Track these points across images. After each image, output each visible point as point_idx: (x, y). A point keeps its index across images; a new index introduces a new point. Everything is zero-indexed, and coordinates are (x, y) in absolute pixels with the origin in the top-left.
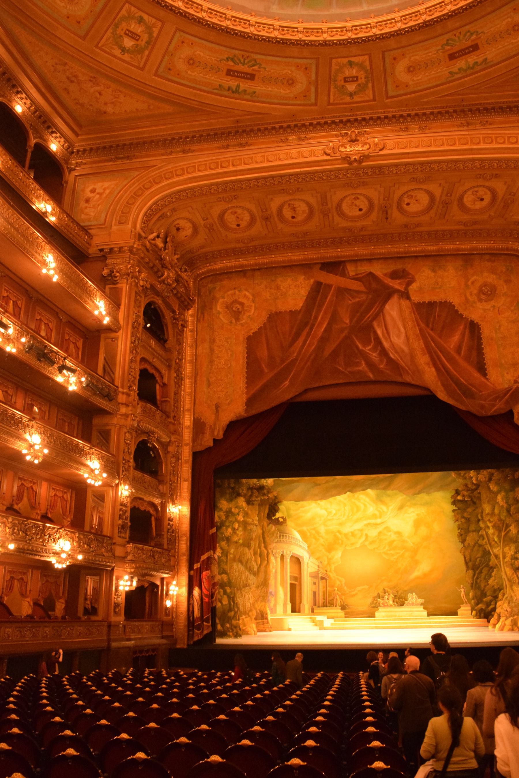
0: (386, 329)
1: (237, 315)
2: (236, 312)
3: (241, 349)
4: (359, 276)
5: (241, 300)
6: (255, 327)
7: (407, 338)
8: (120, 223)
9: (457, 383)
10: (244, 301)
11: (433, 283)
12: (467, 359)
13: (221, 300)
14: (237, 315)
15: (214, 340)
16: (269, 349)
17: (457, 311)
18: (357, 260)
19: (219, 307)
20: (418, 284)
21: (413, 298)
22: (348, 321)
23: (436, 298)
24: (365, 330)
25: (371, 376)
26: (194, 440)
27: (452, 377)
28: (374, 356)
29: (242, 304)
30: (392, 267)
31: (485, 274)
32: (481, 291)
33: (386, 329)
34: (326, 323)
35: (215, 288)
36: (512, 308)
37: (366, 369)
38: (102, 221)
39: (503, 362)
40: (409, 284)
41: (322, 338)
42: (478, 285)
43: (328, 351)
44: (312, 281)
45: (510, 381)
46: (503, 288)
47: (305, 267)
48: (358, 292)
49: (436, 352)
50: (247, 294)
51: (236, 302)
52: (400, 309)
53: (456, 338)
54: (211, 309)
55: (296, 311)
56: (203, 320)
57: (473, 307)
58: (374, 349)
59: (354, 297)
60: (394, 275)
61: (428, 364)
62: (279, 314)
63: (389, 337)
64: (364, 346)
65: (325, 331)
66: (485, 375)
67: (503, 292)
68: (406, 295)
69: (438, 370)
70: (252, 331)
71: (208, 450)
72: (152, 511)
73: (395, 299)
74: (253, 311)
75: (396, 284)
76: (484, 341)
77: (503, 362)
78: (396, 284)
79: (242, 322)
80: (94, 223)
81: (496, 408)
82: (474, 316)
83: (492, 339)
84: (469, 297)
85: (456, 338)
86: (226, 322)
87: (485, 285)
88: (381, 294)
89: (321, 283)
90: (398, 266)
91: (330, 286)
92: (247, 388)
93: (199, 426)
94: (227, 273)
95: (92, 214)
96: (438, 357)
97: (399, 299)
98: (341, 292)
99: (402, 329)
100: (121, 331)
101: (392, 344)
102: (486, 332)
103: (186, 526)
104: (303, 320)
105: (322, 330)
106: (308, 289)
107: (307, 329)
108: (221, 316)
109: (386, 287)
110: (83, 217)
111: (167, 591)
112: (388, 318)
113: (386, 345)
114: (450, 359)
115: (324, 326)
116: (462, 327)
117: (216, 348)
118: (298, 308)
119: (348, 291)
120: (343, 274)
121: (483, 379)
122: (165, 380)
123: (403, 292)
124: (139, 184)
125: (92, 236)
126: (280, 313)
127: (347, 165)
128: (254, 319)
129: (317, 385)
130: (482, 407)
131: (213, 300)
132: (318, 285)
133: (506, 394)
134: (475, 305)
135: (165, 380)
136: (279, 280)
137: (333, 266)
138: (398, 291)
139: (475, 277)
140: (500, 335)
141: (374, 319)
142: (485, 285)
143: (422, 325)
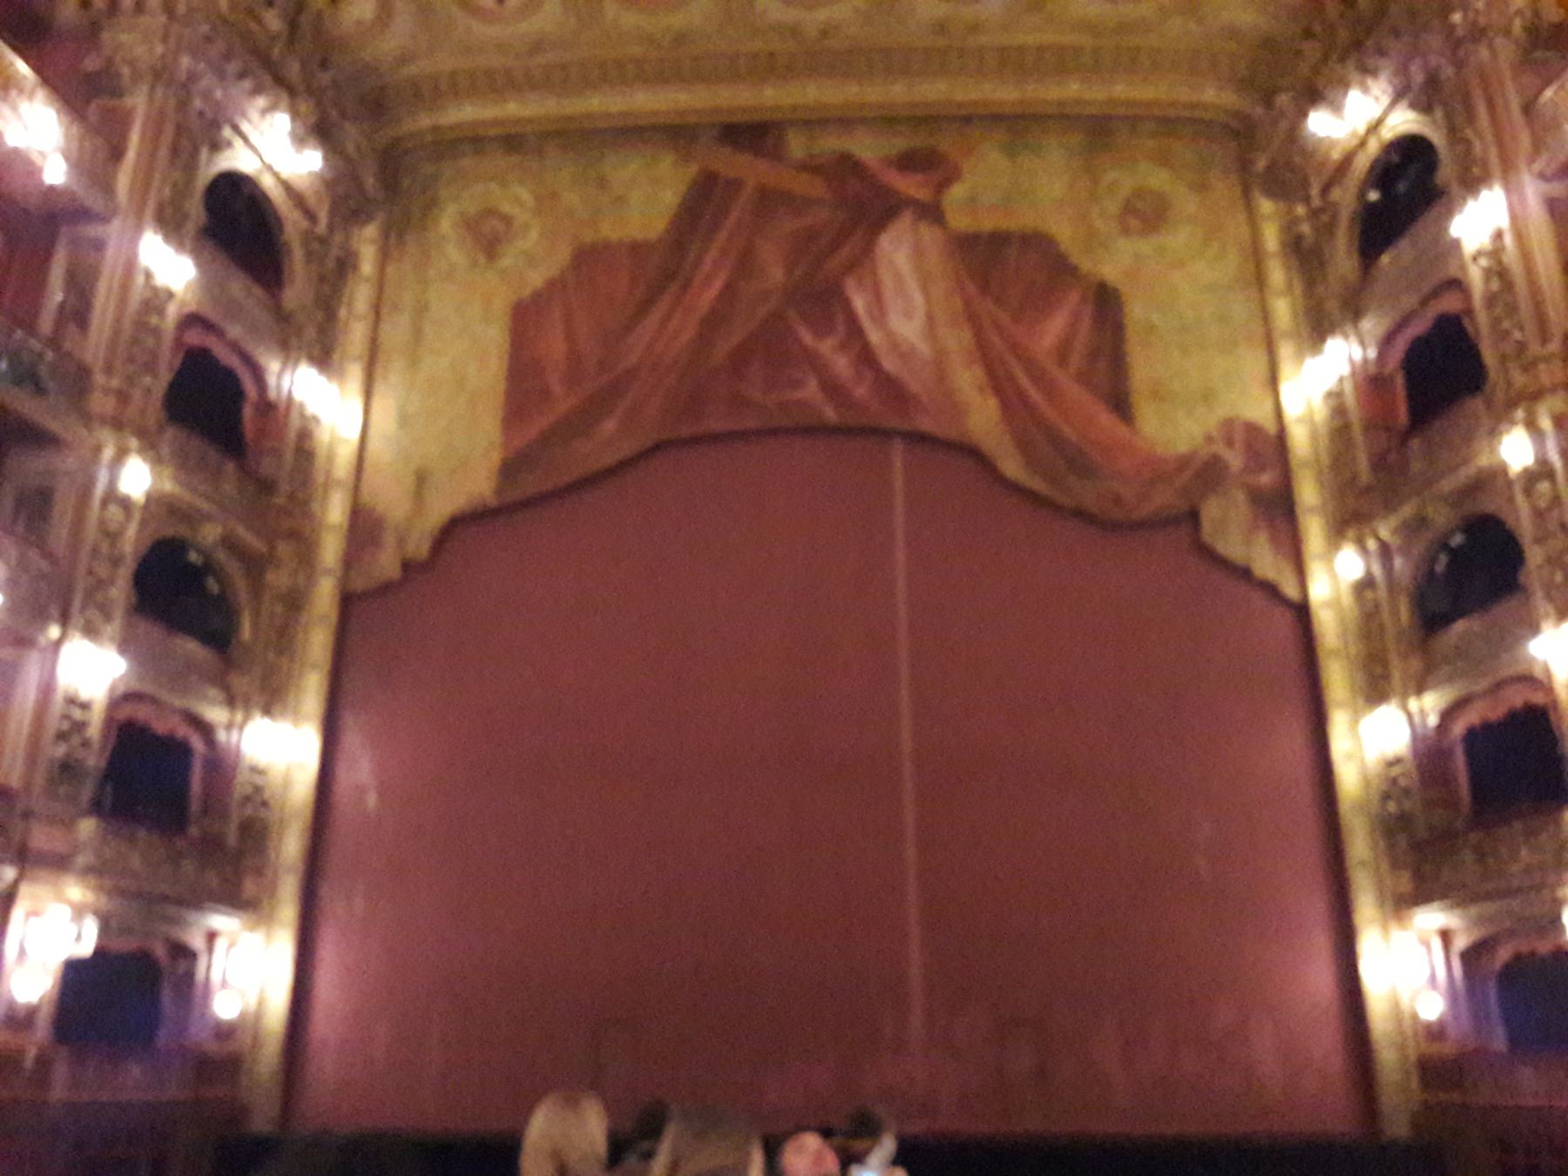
2: (488, 237)
3: (495, 336)
6: (536, 279)
7: (930, 319)
9: (1056, 440)
12: (1084, 378)
16: (570, 337)
18: (815, 121)
19: (446, 222)
24: (822, 300)
26: (350, 560)
28: (842, 365)
29: (507, 220)
30: (899, 144)
32: (1129, 209)
43: (722, 349)
44: (693, 169)
46: (1186, 202)
51: (491, 212)
58: (843, 347)
60: (908, 162)
68: (932, 213)
69: (1006, 406)
75: (911, 186)
85: (1055, 326)
87: (1139, 193)
90: (919, 141)
98: (769, 200)
101: (890, 334)
102: (1136, 312)
104: (663, 266)
107: (674, 288)
113: (874, 336)
114: (1040, 378)
130: (1118, 500)
143: (971, 288)
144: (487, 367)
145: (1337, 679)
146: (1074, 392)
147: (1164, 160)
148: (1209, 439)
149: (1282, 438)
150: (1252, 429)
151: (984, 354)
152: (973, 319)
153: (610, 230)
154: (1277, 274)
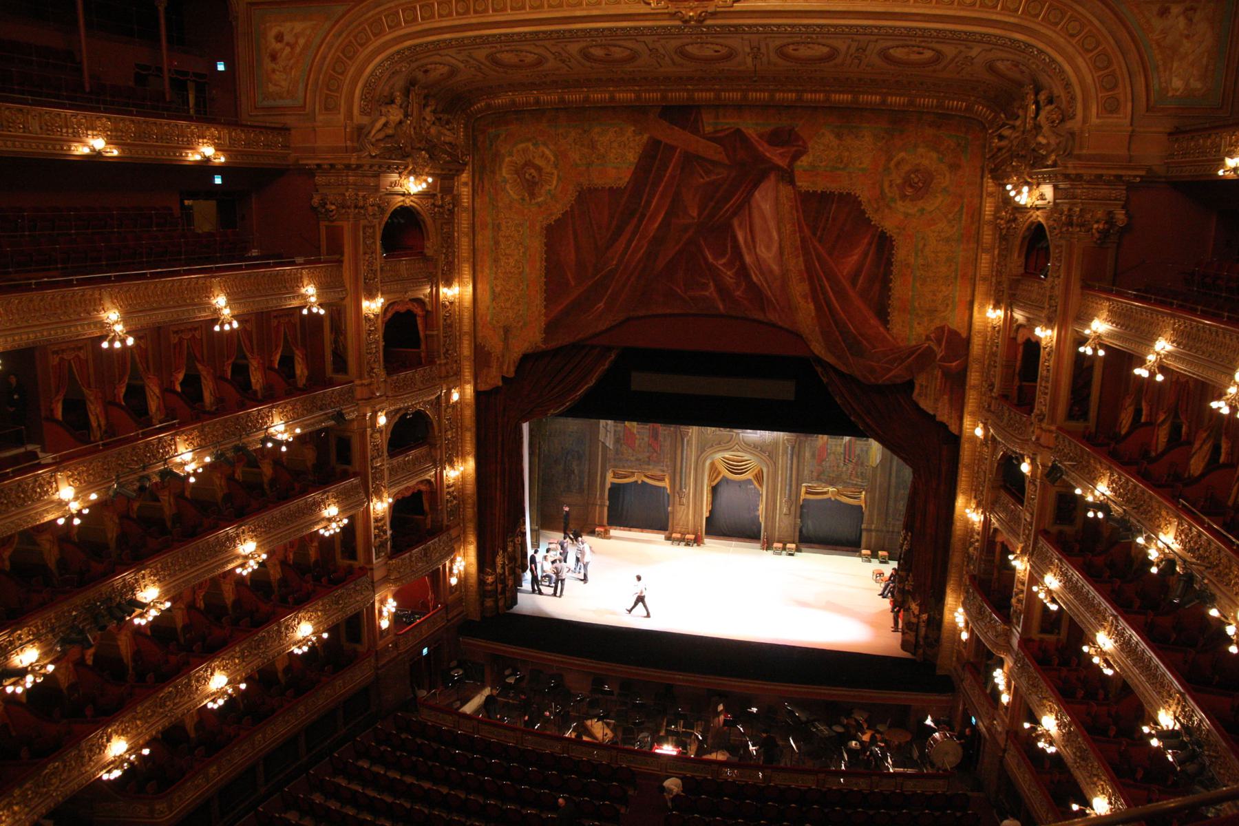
0: (751, 231)
1: (531, 187)
3: (537, 245)
5: (538, 162)
6: (558, 210)
13: (507, 159)
14: (531, 187)
15: (499, 226)
17: (863, 212)
18: (719, 107)
19: (505, 173)
20: (811, 159)
21: (799, 184)
22: (694, 213)
23: (833, 187)
25: (721, 307)
28: (729, 275)
29: (539, 169)
32: (907, 182)
33: (751, 231)
37: (715, 295)
38: (301, 102)
40: (796, 157)
42: (906, 168)
44: (646, 137)
47: (636, 112)
50: (547, 152)
52: (777, 198)
53: (854, 258)
54: (493, 172)
57: (890, 208)
60: (777, 138)
63: (755, 247)
65: (658, 229)
66: (885, 322)
68: (788, 176)
69: (818, 308)
71: (496, 391)
72: (423, 488)
75: (775, 156)
76: (895, 269)
78: (775, 156)
79: (540, 200)
80: (288, 102)
81: (893, 373)
85: (854, 258)
86: (516, 197)
88: (751, 171)
89: (659, 142)
92: (546, 307)
93: (481, 358)
94: (514, 114)
95: (283, 83)
99: (775, 235)
102: (901, 253)
103: (471, 488)
105: (656, 225)
108: (508, 186)
110: (271, 88)
111: (451, 569)
112: (756, 214)
113: (748, 259)
115: (660, 219)
116: (866, 241)
118: (623, 183)
120: (695, 131)
121: (881, 329)
124: (348, 35)
125: (289, 129)
126: (596, 190)
127: (678, 23)
128: (556, 197)
132: (654, 144)
133: (909, 356)
134: (892, 205)
136: (597, 129)
137: (682, 114)
138: (778, 168)
139: (902, 154)
140: (920, 261)
141: (735, 214)
142: (917, 171)
144: (535, 271)
148: (928, 338)
149: (968, 341)
150: (954, 334)
151: (810, 275)
154: (987, 236)
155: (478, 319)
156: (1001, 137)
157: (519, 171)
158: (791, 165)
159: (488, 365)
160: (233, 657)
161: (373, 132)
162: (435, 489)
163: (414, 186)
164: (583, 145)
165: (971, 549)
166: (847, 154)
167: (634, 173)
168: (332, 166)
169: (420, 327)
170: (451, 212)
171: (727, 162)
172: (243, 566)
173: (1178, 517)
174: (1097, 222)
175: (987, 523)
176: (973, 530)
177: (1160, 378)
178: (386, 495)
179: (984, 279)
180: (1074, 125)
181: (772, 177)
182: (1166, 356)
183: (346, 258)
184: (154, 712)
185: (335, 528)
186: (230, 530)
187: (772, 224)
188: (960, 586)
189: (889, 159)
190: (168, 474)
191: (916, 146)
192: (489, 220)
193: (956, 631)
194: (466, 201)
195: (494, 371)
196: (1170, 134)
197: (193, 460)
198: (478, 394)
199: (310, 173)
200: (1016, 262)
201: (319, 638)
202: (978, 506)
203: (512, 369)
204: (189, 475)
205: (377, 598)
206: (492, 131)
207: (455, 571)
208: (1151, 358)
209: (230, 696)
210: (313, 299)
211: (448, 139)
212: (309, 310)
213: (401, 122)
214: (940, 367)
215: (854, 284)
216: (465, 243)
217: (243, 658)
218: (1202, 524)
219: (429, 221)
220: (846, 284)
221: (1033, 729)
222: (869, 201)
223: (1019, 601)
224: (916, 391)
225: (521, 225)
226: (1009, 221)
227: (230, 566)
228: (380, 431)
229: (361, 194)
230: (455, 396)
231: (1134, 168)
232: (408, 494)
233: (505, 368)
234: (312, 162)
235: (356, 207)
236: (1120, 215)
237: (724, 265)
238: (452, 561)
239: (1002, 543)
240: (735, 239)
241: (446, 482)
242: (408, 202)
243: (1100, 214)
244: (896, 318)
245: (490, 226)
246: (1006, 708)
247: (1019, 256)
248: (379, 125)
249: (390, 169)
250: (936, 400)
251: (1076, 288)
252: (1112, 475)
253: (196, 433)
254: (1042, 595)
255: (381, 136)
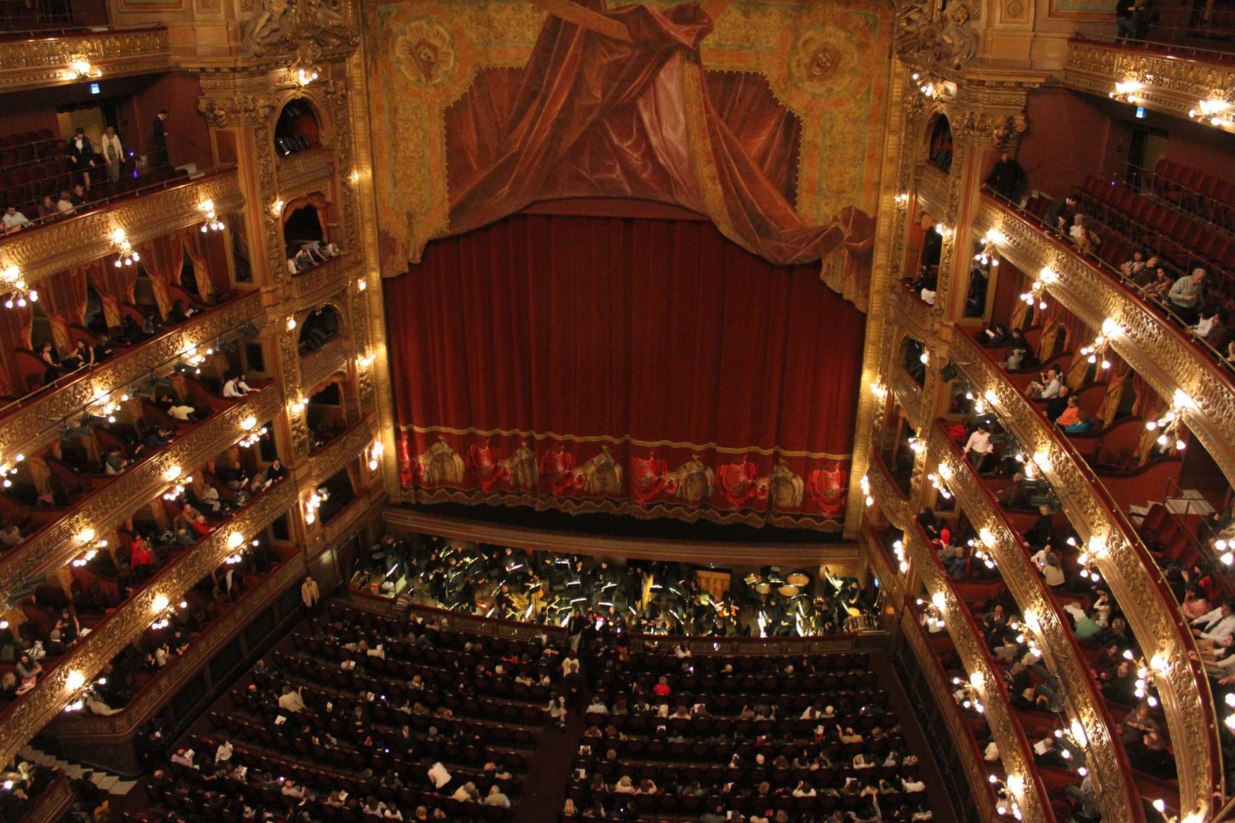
0: (657, 113)
1: (428, 68)
3: (437, 128)
4: (622, 12)
5: (431, 41)
6: (457, 92)
8: (205, 6)
9: (752, 213)
10: (437, 42)
11: (742, 39)
12: (771, 177)
13: (400, 39)
14: (428, 68)
16: (478, 132)
17: (771, 92)
19: (399, 53)
21: (705, 63)
22: (599, 96)
23: (740, 67)
24: (624, 113)
25: (628, 190)
27: (744, 201)
28: (635, 158)
29: (434, 49)
31: (830, 29)
32: (815, 62)
33: (657, 113)
34: (566, 95)
35: (389, 14)
36: (858, 97)
37: (622, 178)
39: (824, 185)
40: (701, 35)
41: (558, 121)
42: (813, 48)
43: (566, 145)
44: (545, 13)
45: (827, 216)
46: (853, 59)
48: (619, 42)
49: (728, 162)
51: (423, 43)
52: (682, 80)
53: (761, 140)
54: (386, 52)
55: (519, 69)
56: (376, 72)
59: (611, 52)
61: (713, 179)
62: (491, 72)
64: (622, 141)
65: (562, 109)
66: (793, 204)
67: (851, 65)
68: (694, 56)
69: (726, 190)
70: (453, 100)
71: (403, 276)
72: (336, 380)
73: (674, 63)
74: (452, 63)
75: (680, 34)
77: (824, 185)
78: (680, 34)
79: (437, 81)
82: (796, 106)
83: (816, 146)
84: (794, 70)
85: (761, 140)
88: (655, 50)
89: (560, 20)
91: (574, 27)
92: (449, 192)
93: (386, 244)
96: (729, 168)
97: (682, 61)
98: (592, 38)
99: (681, 115)
100: (246, 207)
101: (664, 140)
103: (384, 373)
104: (529, 85)
106: (538, 29)
107: (537, 101)
108: (403, 68)
109: (664, 37)
111: (370, 455)
112: (661, 95)
113: (654, 141)
116: (773, 122)
117: (400, 123)
119: (603, 37)
122: (329, 199)
123: (691, 50)
125: (165, 28)
128: (453, 79)
129: (549, 196)
130: (780, 251)
131: (389, 35)
132: (555, 21)
133: (817, 236)
134: (800, 85)
135: (329, 199)
138: (681, 47)
140: (828, 142)
141: (640, 94)
142: (825, 50)
143: (714, 113)
145: (870, 355)
146: (766, 184)
147: (843, 23)
148: (835, 219)
149: (873, 223)
150: (860, 213)
151: (717, 156)
152: (713, 133)
153: (498, 61)
154: (895, 118)
155: (380, 205)
156: (909, 21)
157: (413, 51)
158: (696, 44)
159: (393, 251)
160: (170, 578)
161: (257, 30)
162: (349, 378)
163: (304, 78)
164: (478, 24)
165: (876, 422)
166: (754, 32)
167: (534, 53)
168: (217, 70)
169: (321, 220)
170: (345, 97)
171: (631, 41)
172: (170, 491)
173: (1051, 438)
174: (997, 128)
175: (890, 398)
176: (877, 403)
177: (1043, 306)
178: (300, 396)
179: (890, 160)
180: (979, 26)
181: (678, 57)
182: (1050, 286)
183: (240, 166)
184: (104, 643)
185: (254, 438)
186: (155, 460)
187: (678, 107)
188: (865, 455)
189: (797, 39)
190: (88, 420)
191: (824, 24)
192: (385, 102)
193: (862, 498)
194: (358, 84)
195: (400, 257)
196: (1070, 40)
197: (111, 400)
198: (385, 281)
199: (195, 76)
200: (922, 149)
201: (251, 547)
202: (883, 381)
203: (418, 256)
204: (108, 416)
205: (301, 495)
206: (382, 8)
207: (374, 455)
208: (1036, 286)
209: (173, 615)
210: (211, 215)
211: (336, 23)
212: (208, 227)
213: (285, 12)
214: (847, 247)
215: (761, 166)
216: (359, 129)
217: (180, 577)
218: (1070, 451)
219: (322, 110)
220: (754, 165)
221: (925, 605)
222: (776, 82)
223: (917, 481)
224: (824, 270)
225: (419, 107)
226: (915, 106)
227: (158, 494)
228: (290, 333)
229: (250, 97)
230: (362, 286)
231: (1032, 76)
232: (322, 389)
233: (411, 254)
234: (193, 66)
235: (246, 111)
236: (1020, 121)
237: (629, 147)
238: (371, 448)
239: (904, 419)
240: (640, 120)
241: (359, 372)
242: (300, 95)
243: (1000, 120)
244: (805, 202)
245: (386, 109)
246: (905, 576)
247: (925, 142)
248: (262, 21)
249: (278, 65)
250: (844, 279)
251: (976, 195)
252: (1000, 383)
253: (109, 372)
254: (936, 485)
255: (266, 32)
